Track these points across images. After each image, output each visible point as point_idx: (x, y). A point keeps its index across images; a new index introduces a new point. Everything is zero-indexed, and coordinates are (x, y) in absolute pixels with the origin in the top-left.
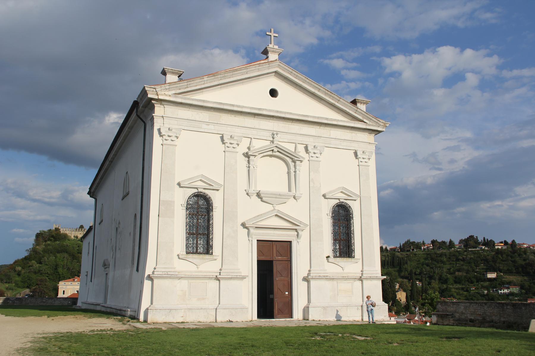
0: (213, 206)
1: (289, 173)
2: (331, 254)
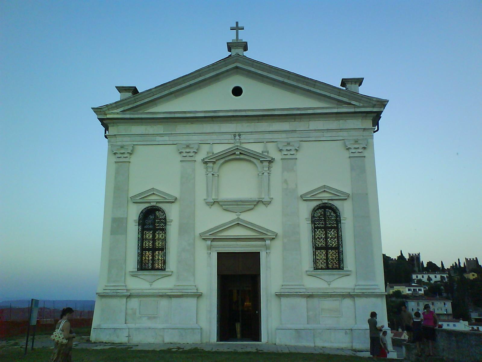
0: (167, 219)
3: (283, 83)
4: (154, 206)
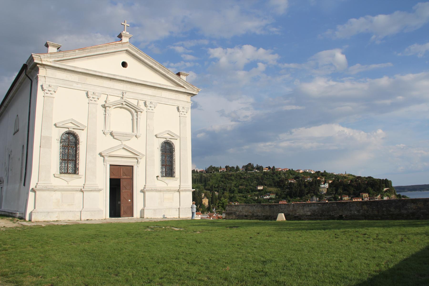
1: (133, 120)
2: (159, 174)
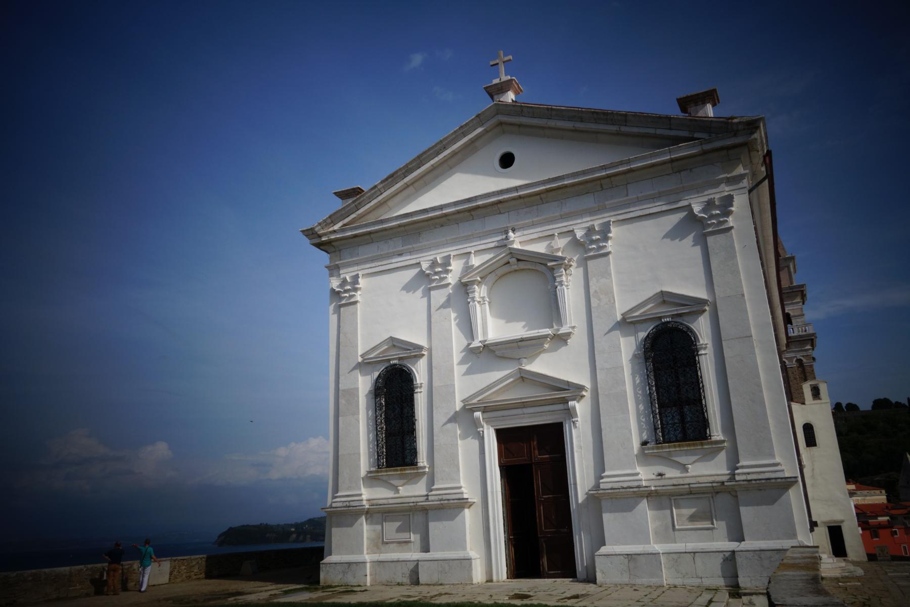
3: (575, 131)
4: (395, 365)
